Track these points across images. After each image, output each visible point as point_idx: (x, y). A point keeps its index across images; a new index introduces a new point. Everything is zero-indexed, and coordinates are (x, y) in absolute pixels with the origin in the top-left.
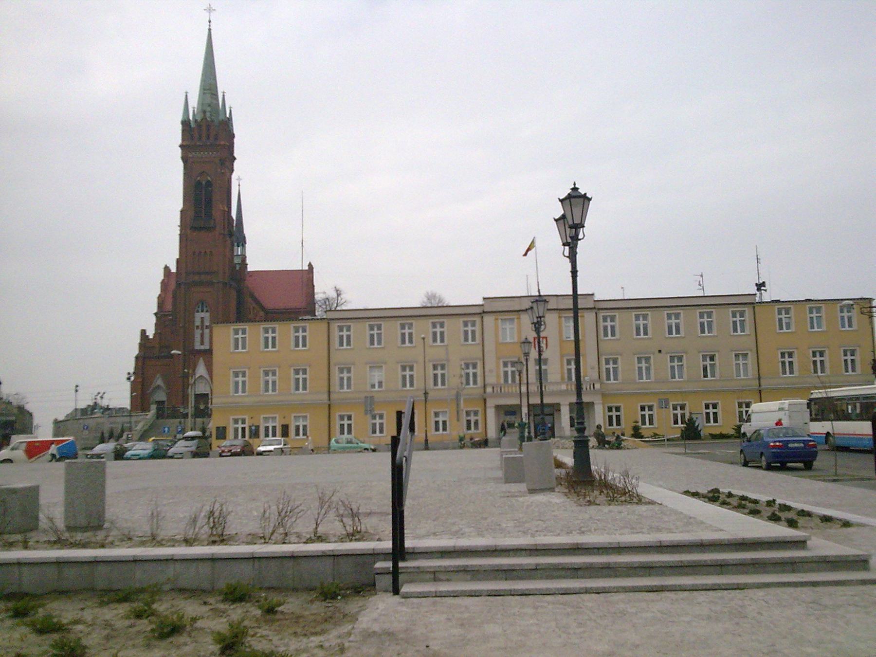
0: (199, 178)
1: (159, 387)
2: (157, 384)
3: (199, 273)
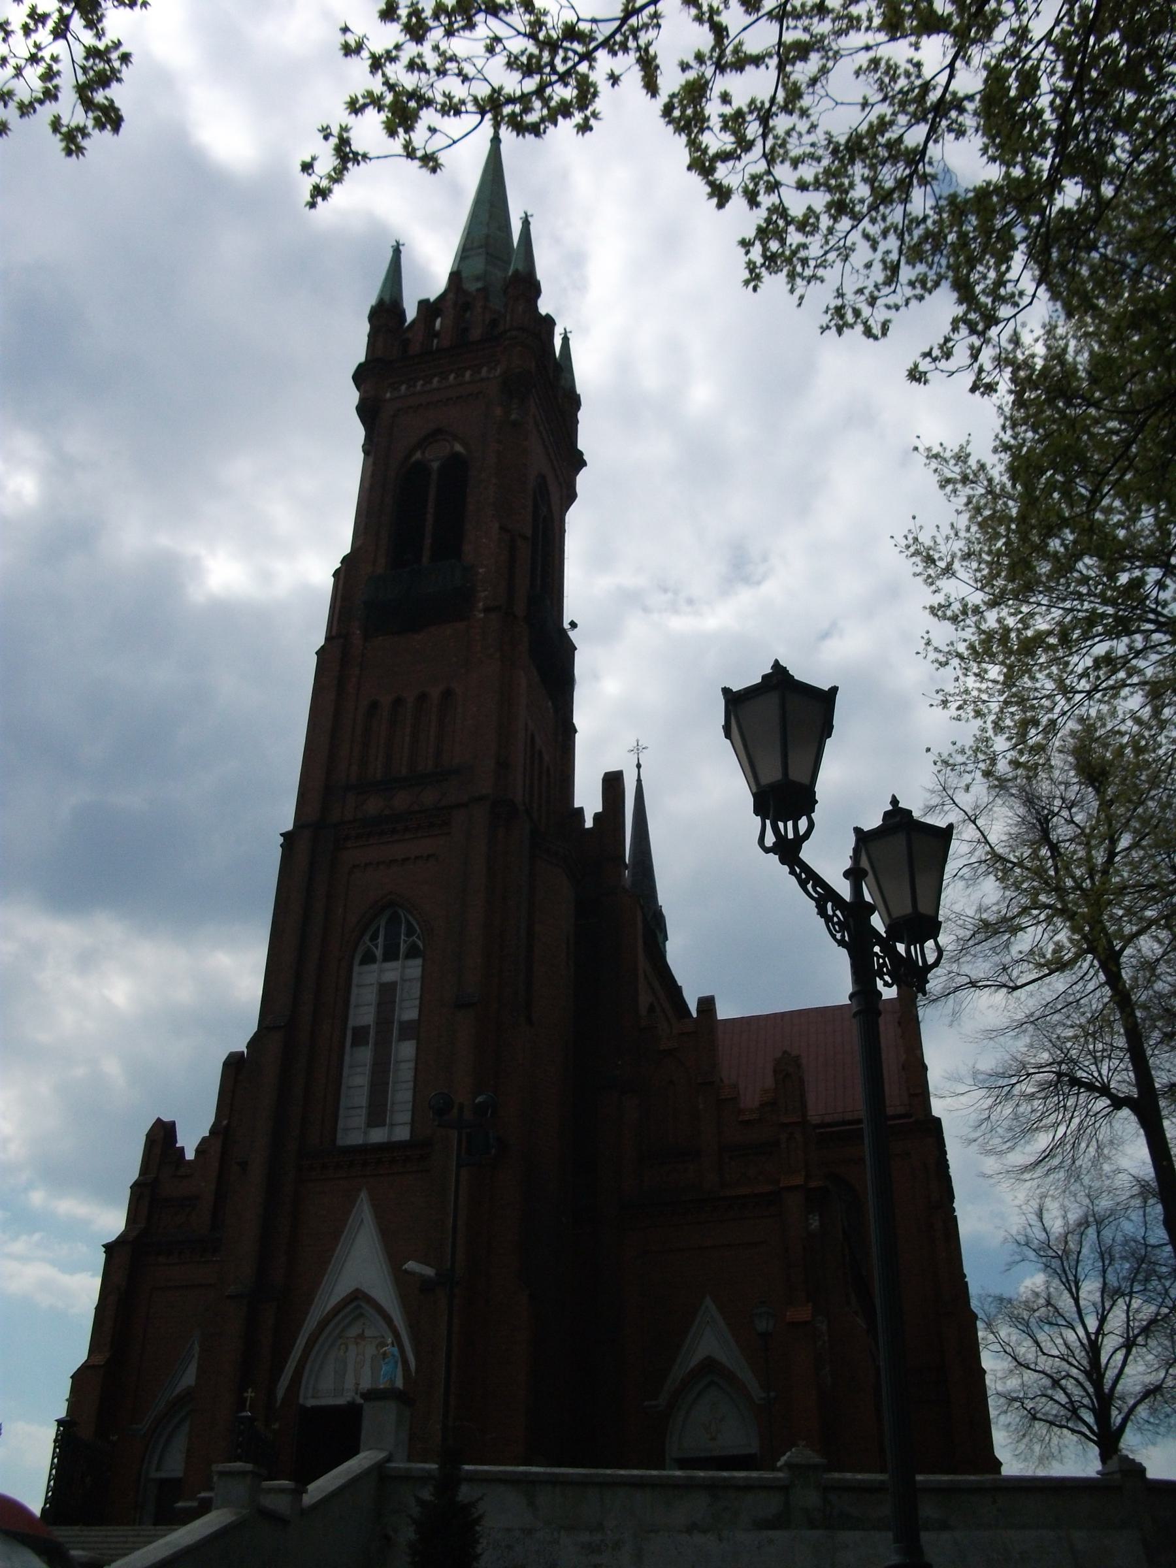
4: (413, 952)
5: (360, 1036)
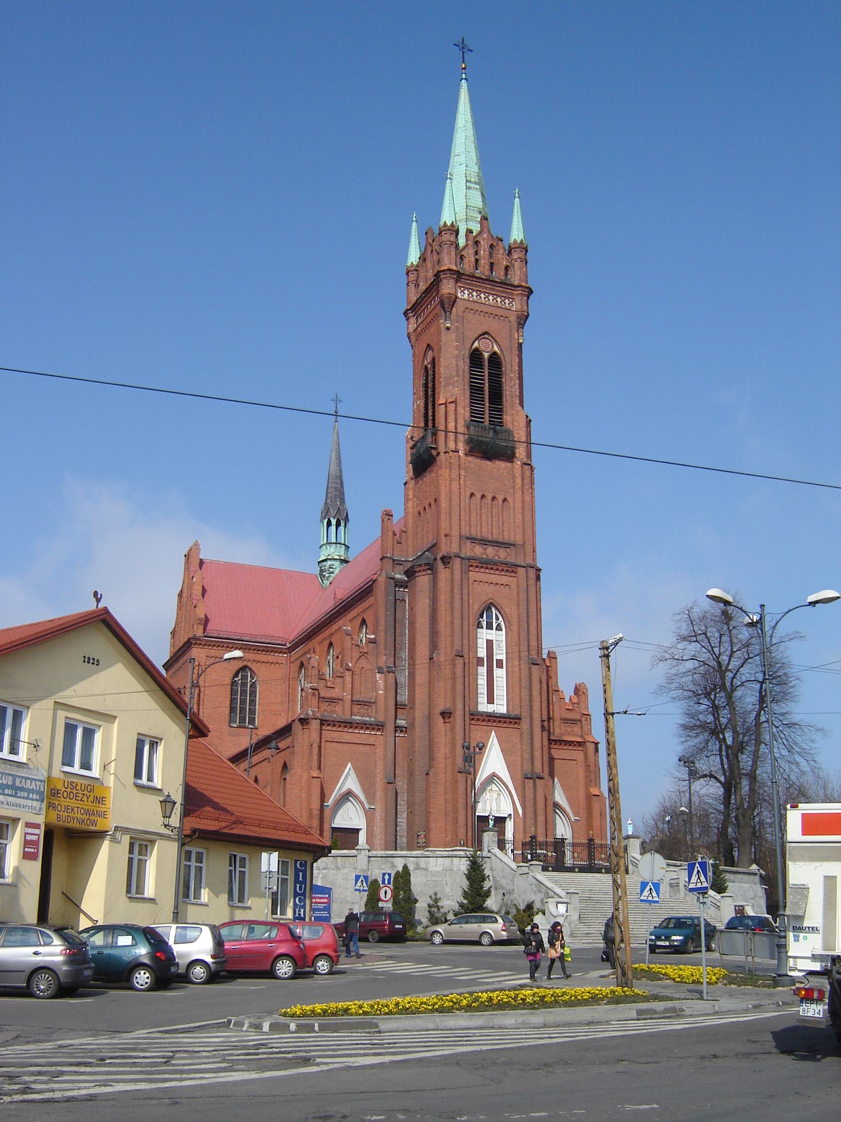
0: (476, 344)
1: (348, 795)
2: (344, 790)
3: (484, 542)
4: (499, 628)
5: (480, 661)
